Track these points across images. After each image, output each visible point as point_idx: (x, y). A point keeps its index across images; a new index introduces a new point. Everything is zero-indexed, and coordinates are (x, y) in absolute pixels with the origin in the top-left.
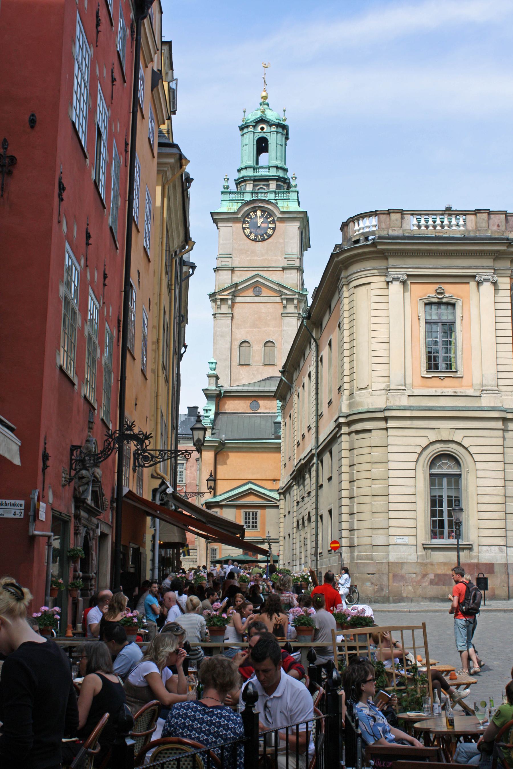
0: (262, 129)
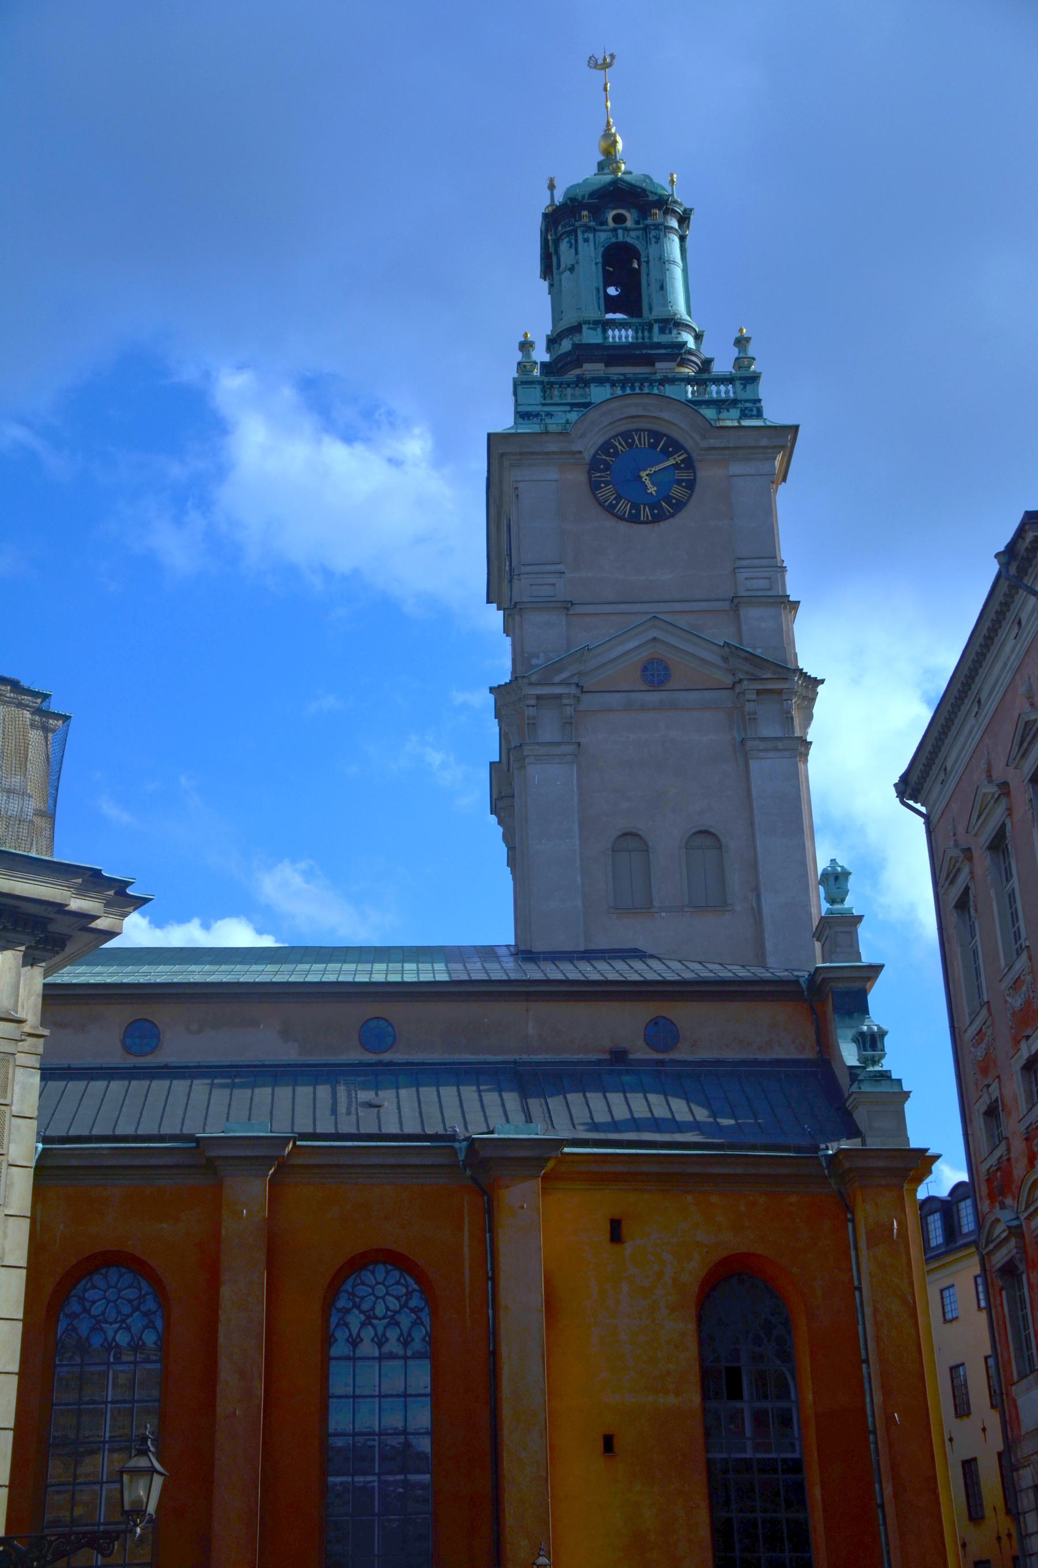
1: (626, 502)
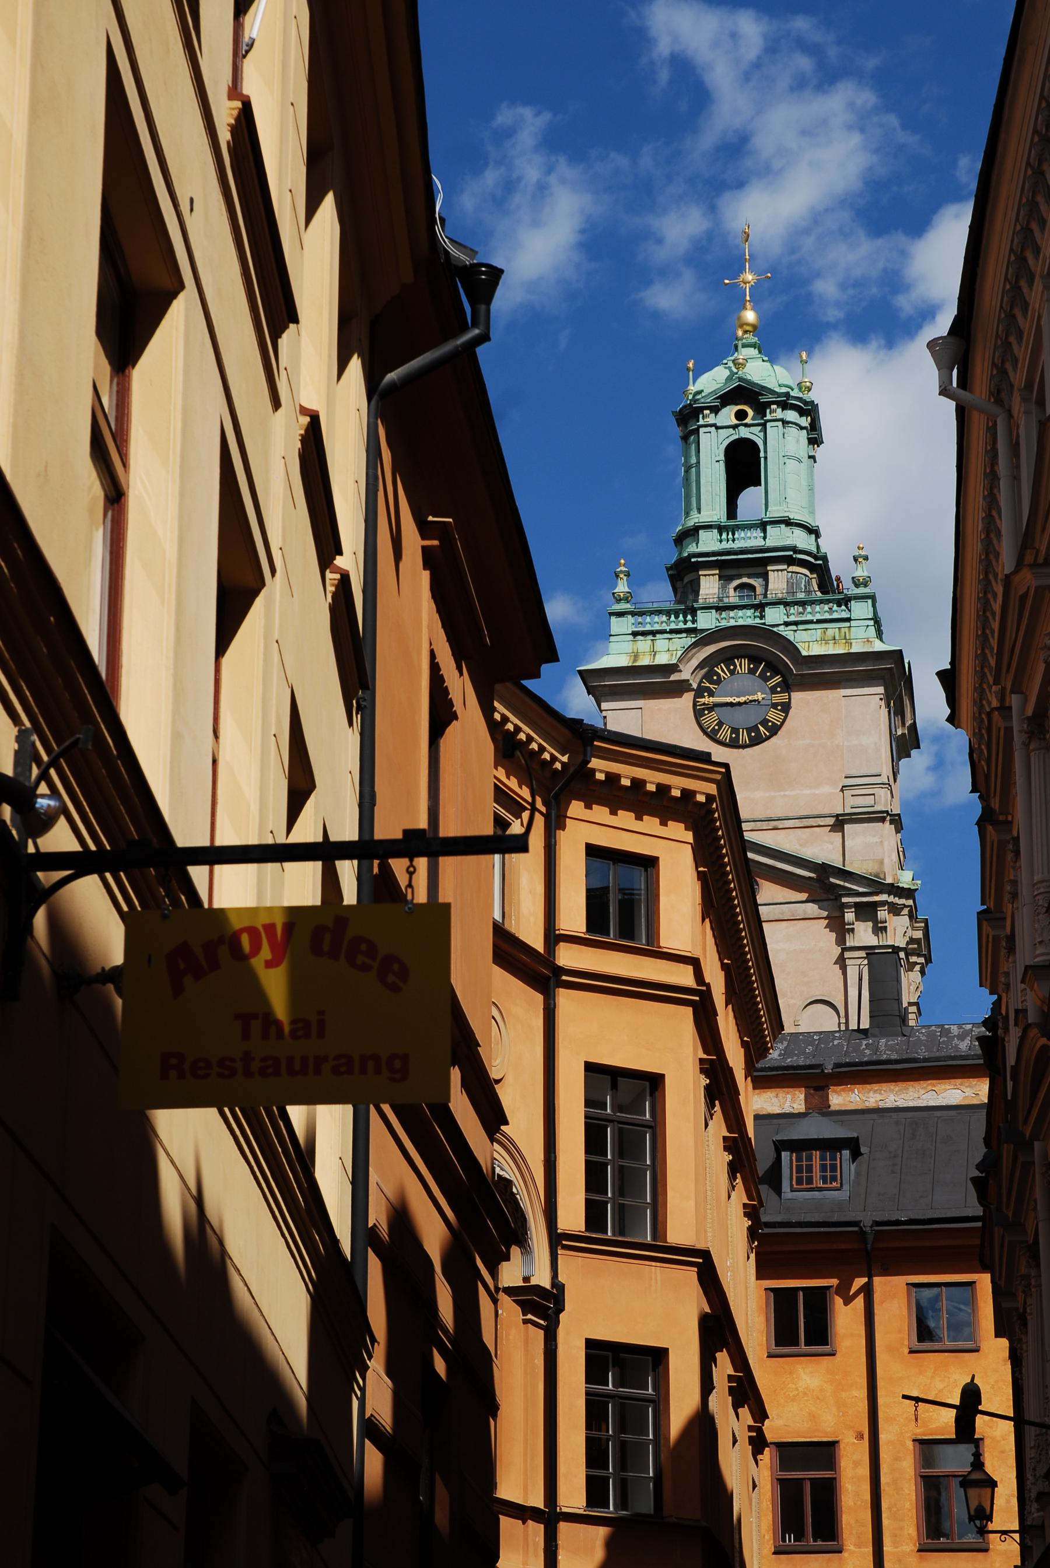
0: (741, 415)
1: (728, 727)
